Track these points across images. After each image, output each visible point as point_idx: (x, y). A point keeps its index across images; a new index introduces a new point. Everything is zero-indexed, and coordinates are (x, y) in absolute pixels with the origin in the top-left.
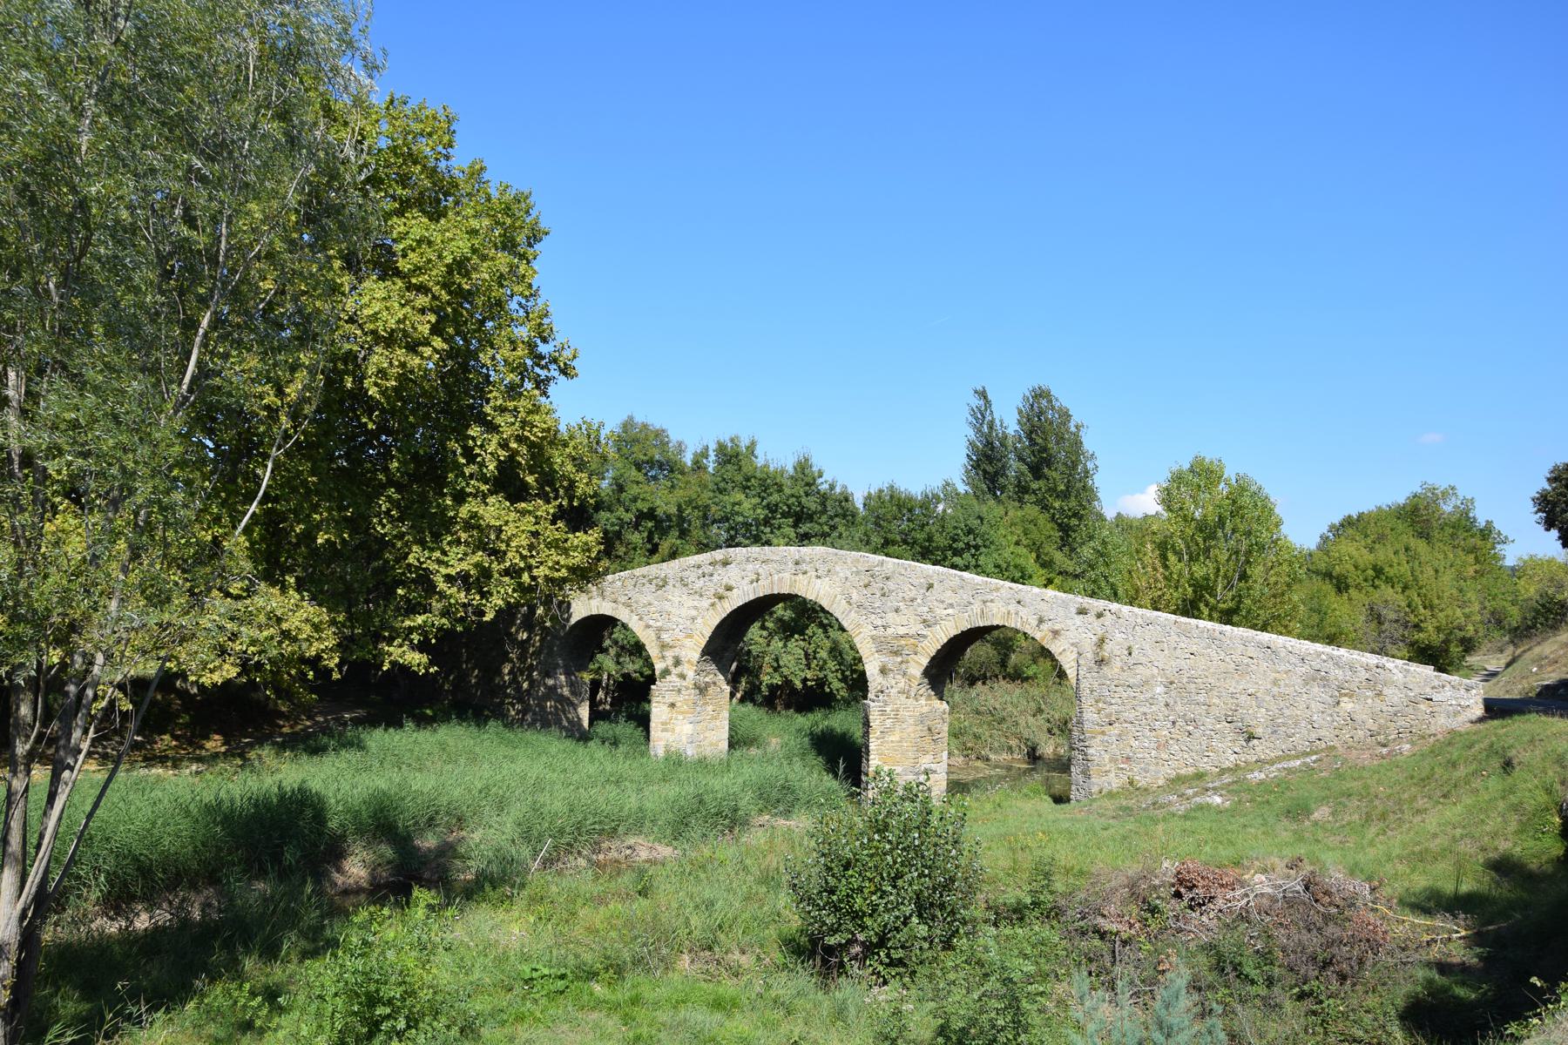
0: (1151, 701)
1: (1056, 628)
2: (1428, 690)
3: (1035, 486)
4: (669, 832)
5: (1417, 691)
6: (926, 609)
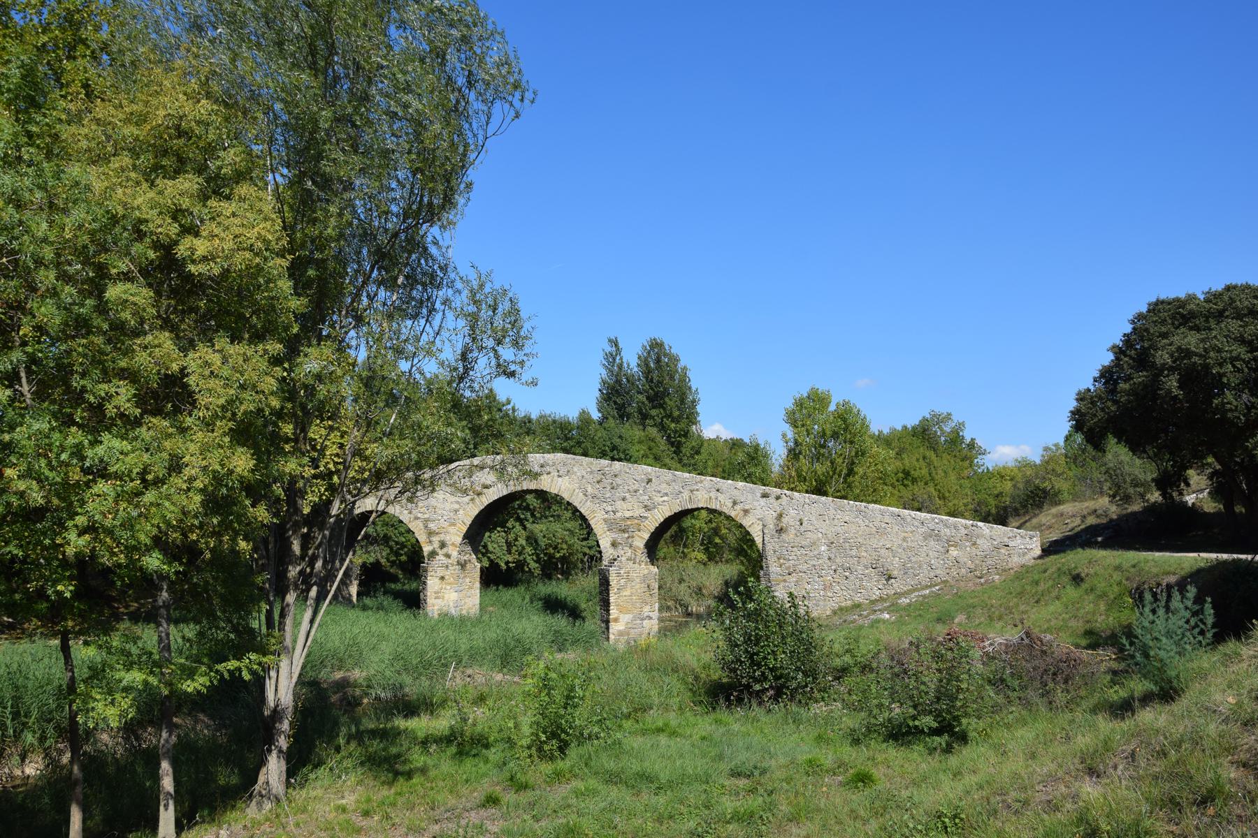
0: (819, 556)
1: (747, 507)
2: (1006, 539)
3: (654, 412)
4: (498, 662)
5: (999, 540)
6: (647, 497)
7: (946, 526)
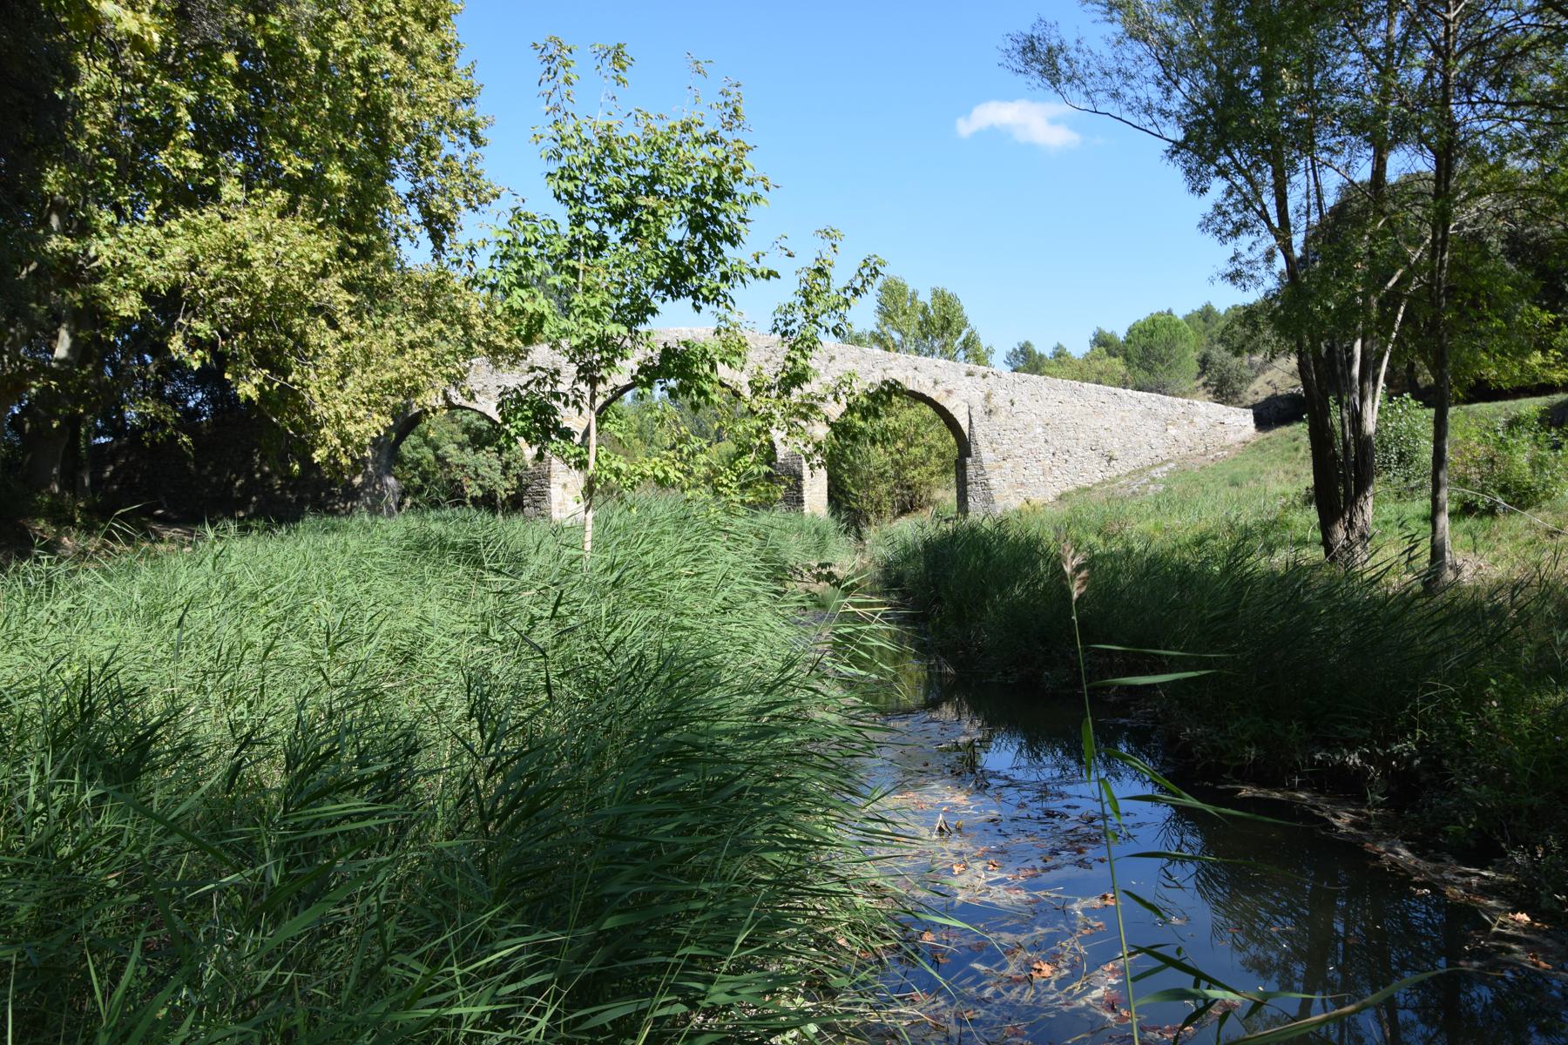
0: (1034, 439)
1: (950, 387)
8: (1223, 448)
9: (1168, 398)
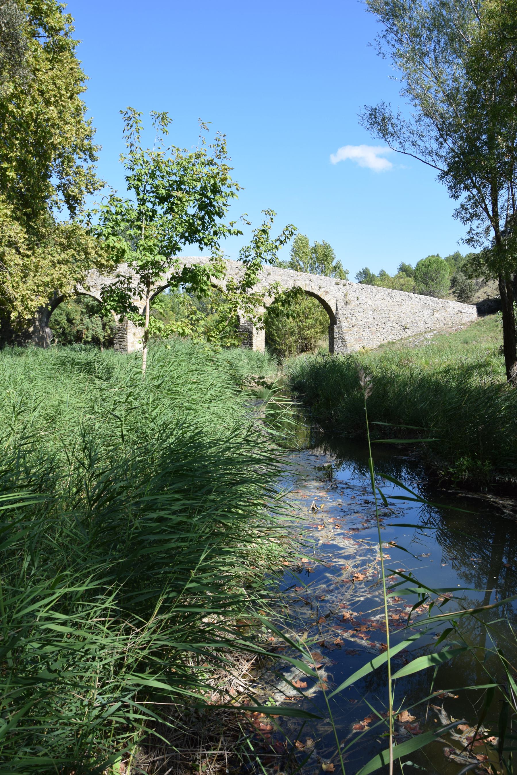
1: (327, 290)
7: (432, 302)
8: (461, 324)
9: (435, 299)
